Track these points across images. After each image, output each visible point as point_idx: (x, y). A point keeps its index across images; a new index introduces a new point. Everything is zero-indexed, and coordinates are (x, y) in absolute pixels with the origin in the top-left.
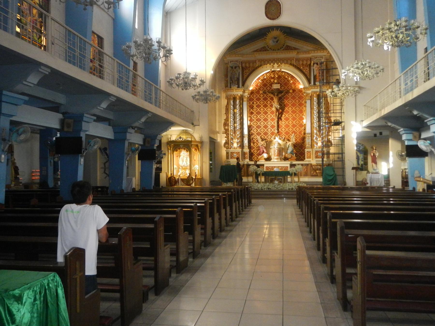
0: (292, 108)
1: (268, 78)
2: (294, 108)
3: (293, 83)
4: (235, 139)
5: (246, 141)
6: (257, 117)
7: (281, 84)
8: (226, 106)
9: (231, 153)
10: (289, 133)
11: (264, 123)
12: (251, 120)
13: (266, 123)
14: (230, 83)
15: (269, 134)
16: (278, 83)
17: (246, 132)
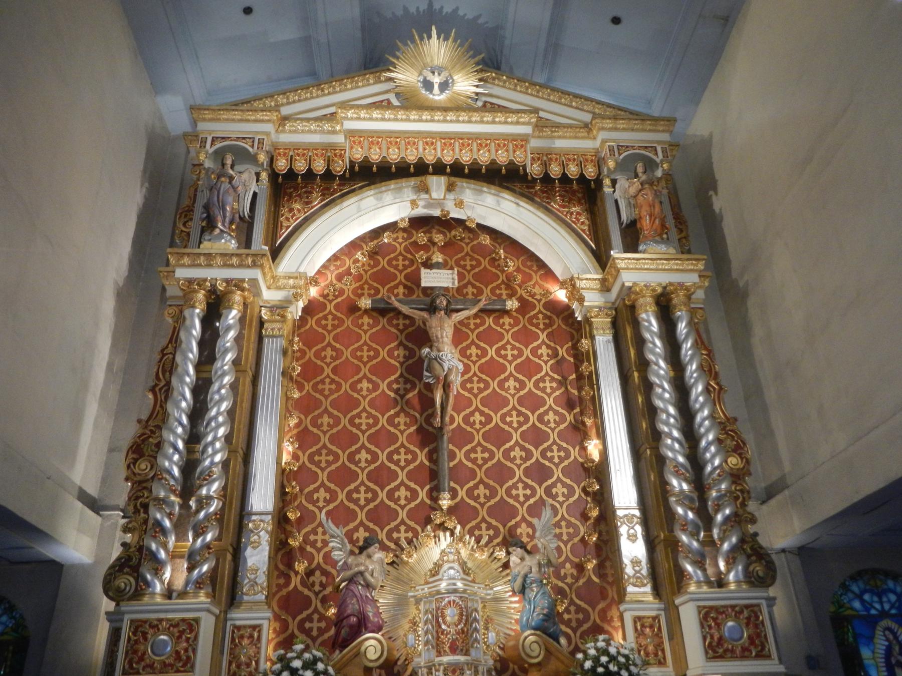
0: (522, 385)
1: (400, 248)
2: (530, 385)
3: (518, 270)
4: (181, 537)
5: (258, 557)
6: (337, 421)
7: (461, 276)
8: (163, 353)
9: (138, 626)
10: (514, 512)
11: (375, 457)
12: (303, 438)
13: (383, 457)
14: (203, 231)
15: (403, 514)
16: (452, 268)
17: (262, 498)
